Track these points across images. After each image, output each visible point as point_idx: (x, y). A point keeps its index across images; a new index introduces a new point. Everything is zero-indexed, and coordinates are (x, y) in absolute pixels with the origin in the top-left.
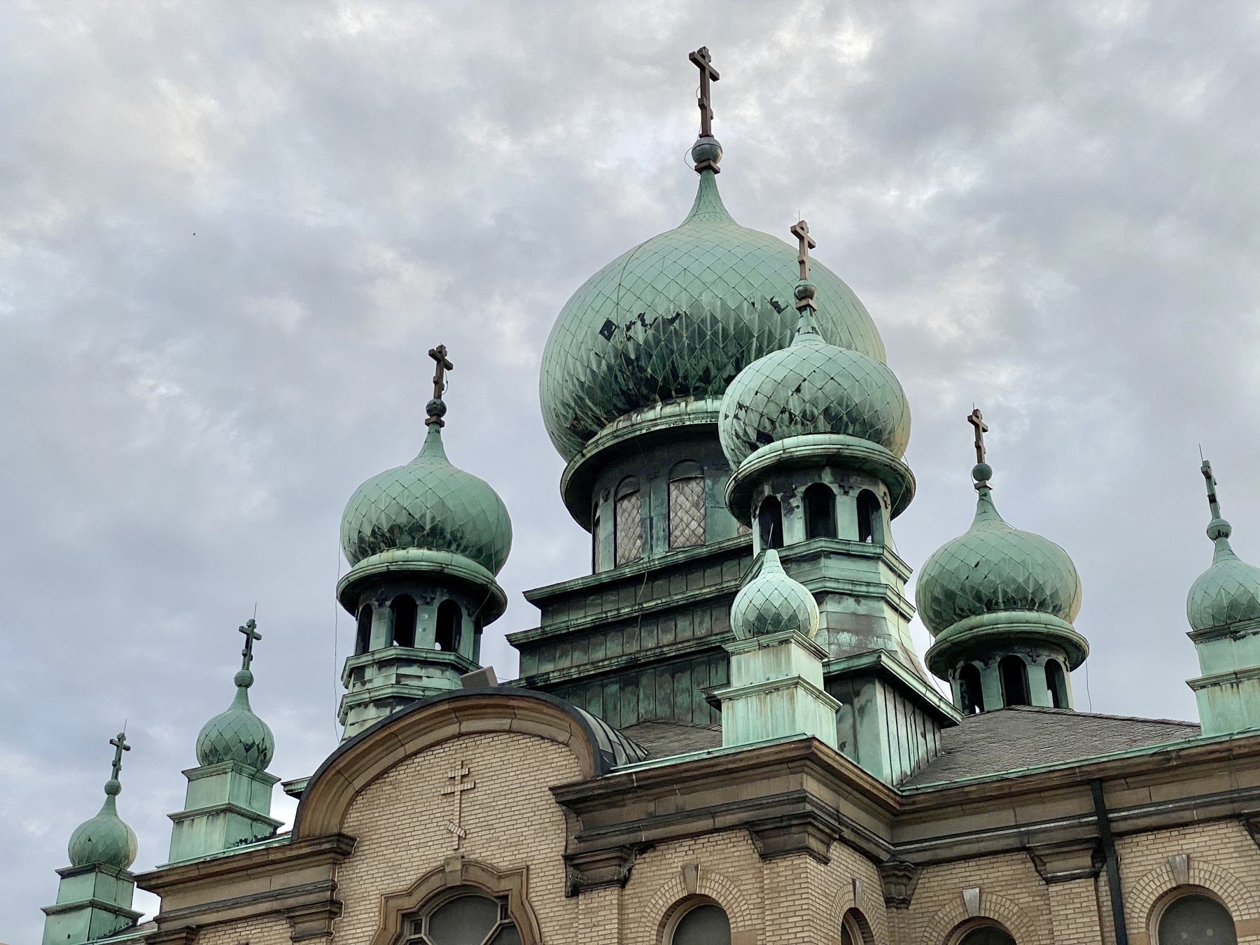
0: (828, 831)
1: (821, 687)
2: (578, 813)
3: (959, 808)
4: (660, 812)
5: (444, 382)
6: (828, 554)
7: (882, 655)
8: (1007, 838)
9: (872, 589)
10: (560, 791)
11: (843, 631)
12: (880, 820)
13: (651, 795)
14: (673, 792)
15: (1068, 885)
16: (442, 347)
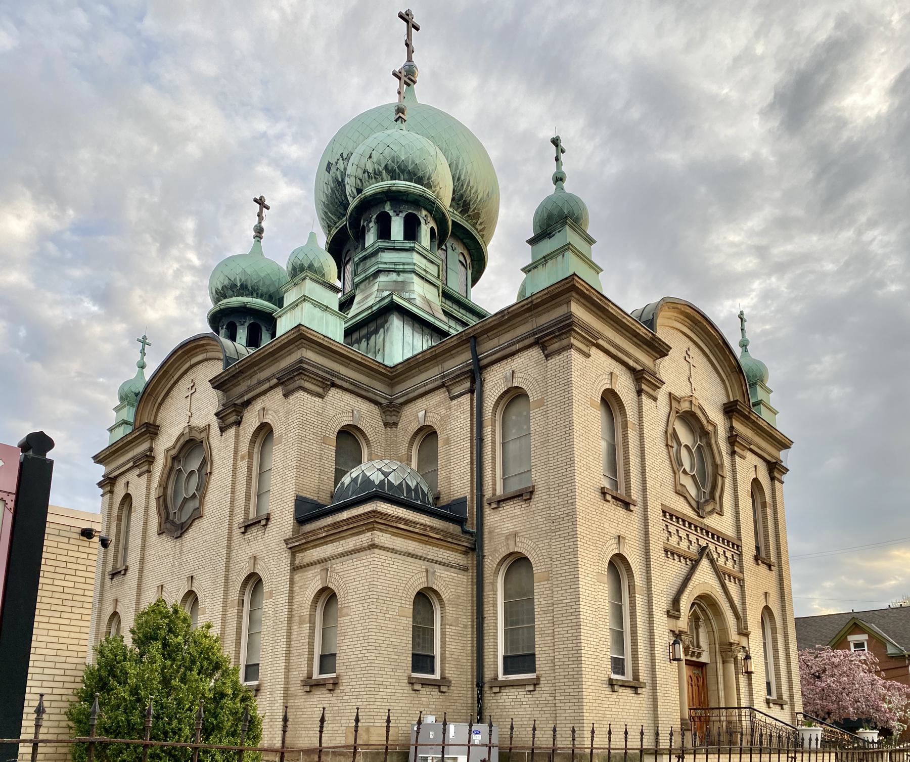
0: (320, 379)
1: (337, 309)
2: (226, 392)
3: (417, 369)
4: (253, 384)
5: (264, 215)
6: (383, 250)
7: (394, 296)
8: (437, 380)
9: (406, 267)
10: (214, 381)
11: (386, 291)
12: (384, 384)
13: (248, 376)
14: (255, 373)
15: (459, 399)
16: (262, 197)
